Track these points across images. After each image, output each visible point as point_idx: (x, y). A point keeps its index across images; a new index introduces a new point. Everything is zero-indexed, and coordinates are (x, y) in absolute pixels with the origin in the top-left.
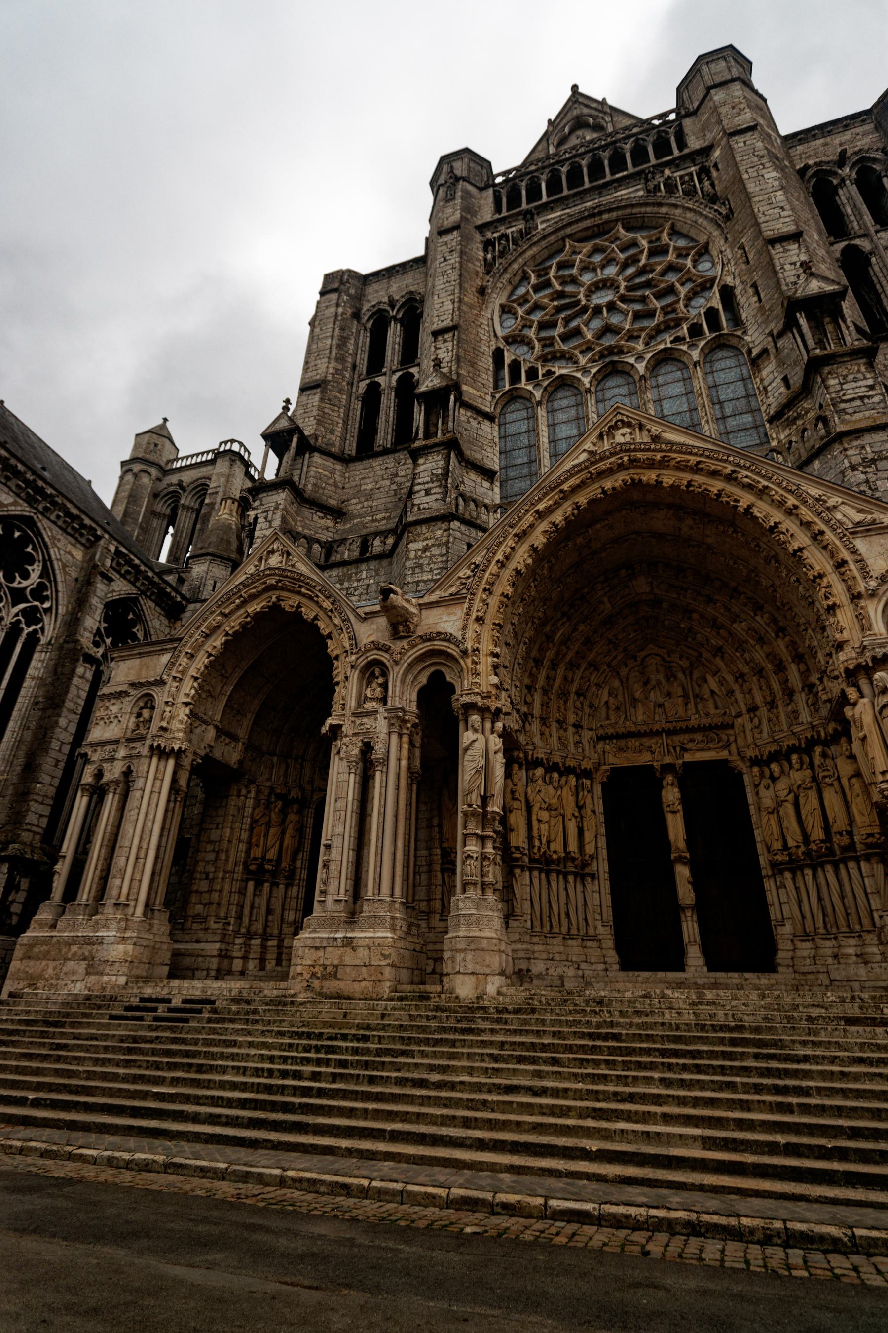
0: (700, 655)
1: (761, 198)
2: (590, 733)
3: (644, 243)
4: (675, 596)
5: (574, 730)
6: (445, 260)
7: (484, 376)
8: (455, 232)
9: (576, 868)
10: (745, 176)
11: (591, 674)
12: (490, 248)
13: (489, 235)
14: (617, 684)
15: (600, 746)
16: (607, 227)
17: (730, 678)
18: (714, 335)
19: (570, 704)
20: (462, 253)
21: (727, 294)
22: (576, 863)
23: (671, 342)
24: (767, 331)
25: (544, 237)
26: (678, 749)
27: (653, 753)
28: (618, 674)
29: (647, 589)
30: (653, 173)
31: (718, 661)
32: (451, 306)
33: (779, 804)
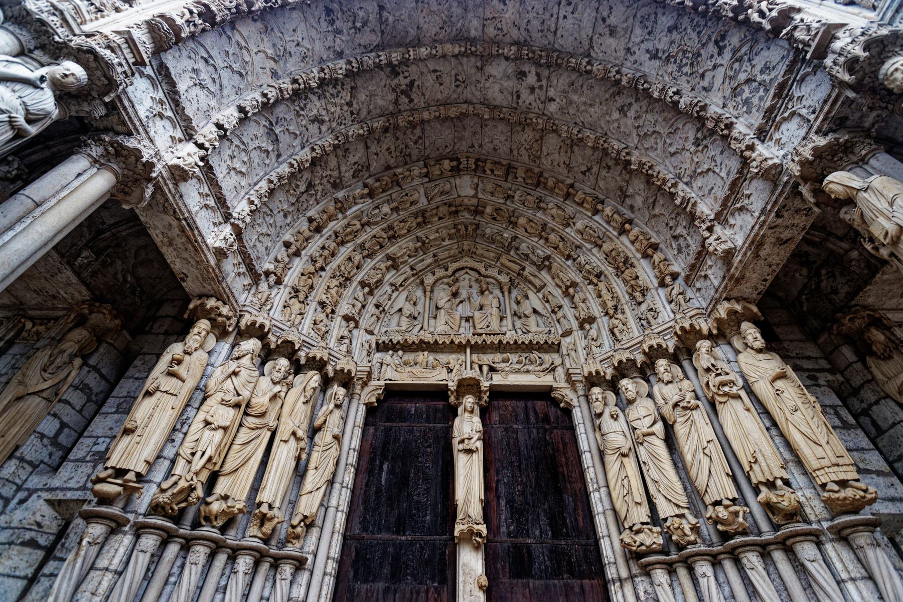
0: (523, 269)
2: (369, 337)
4: (502, 201)
5: (344, 323)
9: (266, 540)
11: (388, 269)
14: (419, 293)
15: (377, 357)
17: (558, 292)
19: (348, 292)
22: (268, 528)
26: (485, 369)
27: (450, 371)
28: (422, 282)
29: (472, 192)
31: (545, 275)
33: (638, 442)
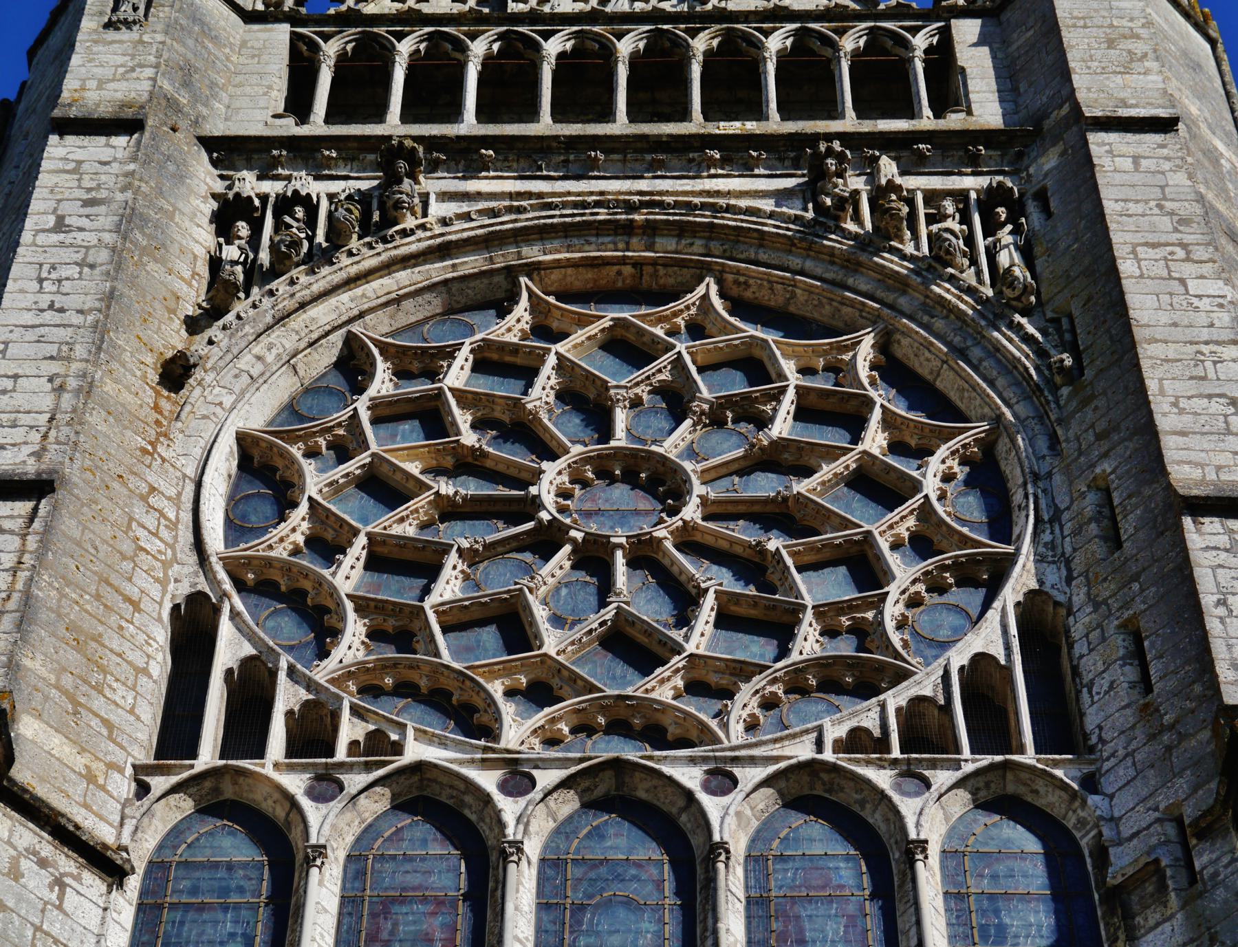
1: (1171, 351)
3: (789, 367)
6: (60, 225)
7: (122, 695)
8: (121, 141)
10: (1126, 267)
12: (243, 229)
13: (249, 184)
16: (668, 279)
18: (986, 760)
20: (129, 220)
21: (1040, 627)
23: (839, 746)
24: (1163, 801)
25: (444, 251)
30: (840, 157)
32: (47, 402)
